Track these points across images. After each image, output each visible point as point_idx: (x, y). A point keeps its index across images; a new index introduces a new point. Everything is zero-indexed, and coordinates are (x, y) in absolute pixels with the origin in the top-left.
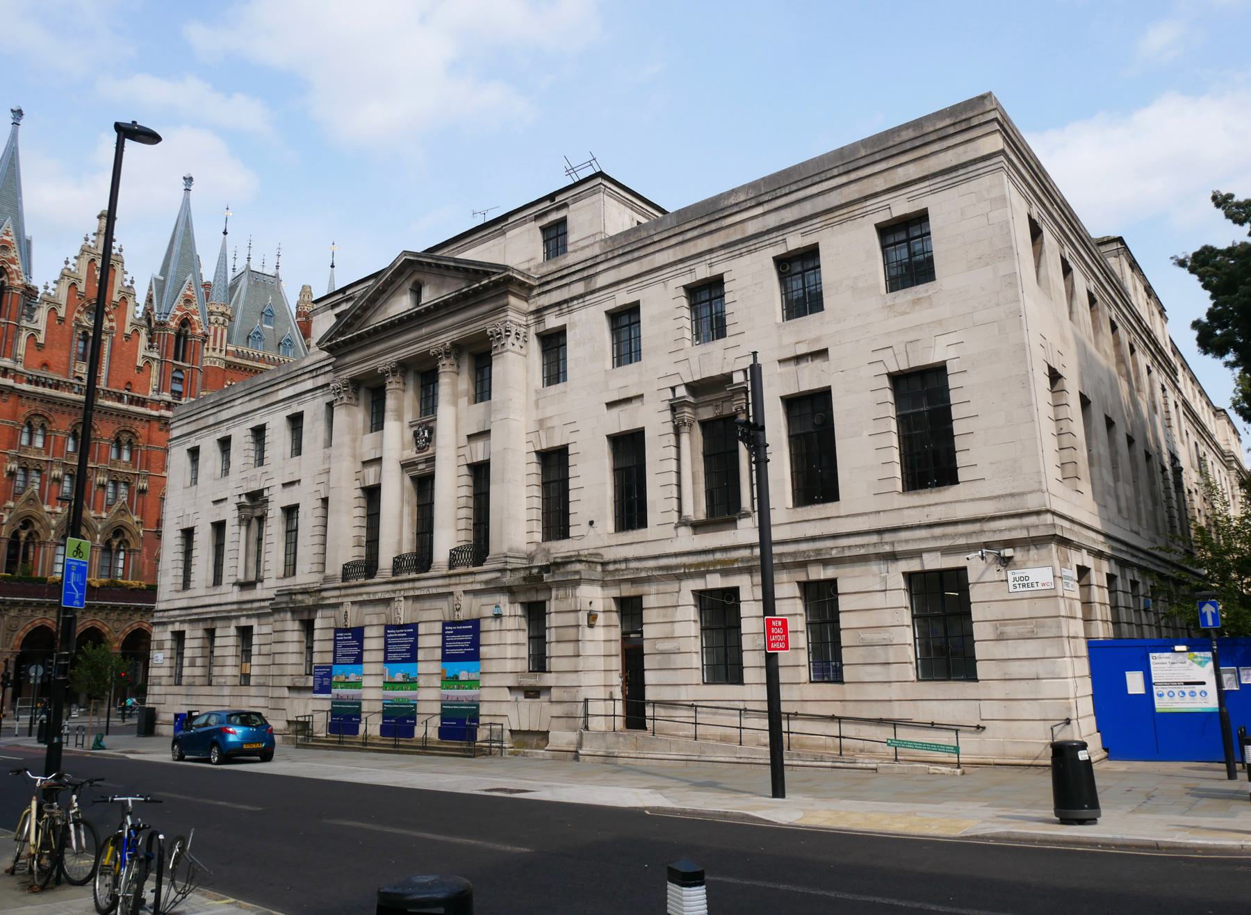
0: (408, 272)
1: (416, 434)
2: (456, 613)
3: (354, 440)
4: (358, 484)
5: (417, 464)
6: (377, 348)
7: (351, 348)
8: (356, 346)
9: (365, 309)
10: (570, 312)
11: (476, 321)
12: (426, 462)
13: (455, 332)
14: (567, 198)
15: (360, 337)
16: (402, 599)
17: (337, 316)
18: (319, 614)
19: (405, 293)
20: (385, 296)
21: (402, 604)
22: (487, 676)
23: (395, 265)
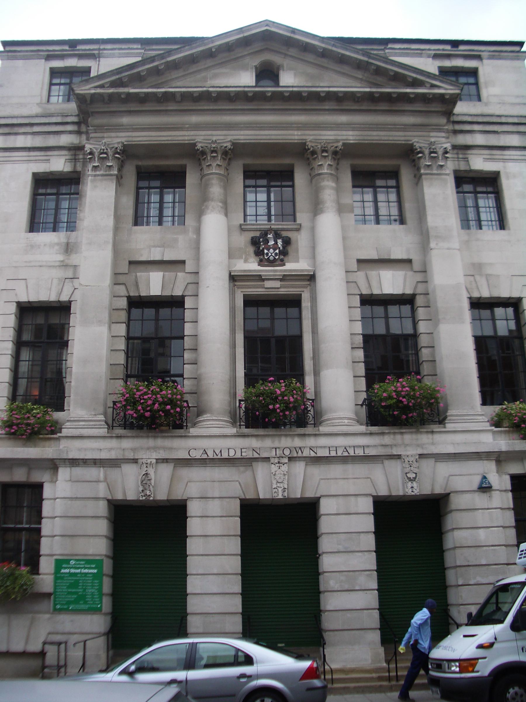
0: (257, 46)
1: (255, 242)
2: (410, 484)
3: (117, 229)
4: (122, 290)
5: (263, 280)
6: (194, 119)
7: (133, 107)
8: (147, 107)
9: (175, 66)
10: (504, 160)
11: (390, 130)
12: (281, 280)
13: (351, 133)
14: (483, 51)
15: (168, 97)
16: (286, 460)
17: (54, 73)
18: (63, 473)
19: (245, 68)
20: (209, 62)
21: (285, 468)
22: (472, 570)
23: (251, 30)
